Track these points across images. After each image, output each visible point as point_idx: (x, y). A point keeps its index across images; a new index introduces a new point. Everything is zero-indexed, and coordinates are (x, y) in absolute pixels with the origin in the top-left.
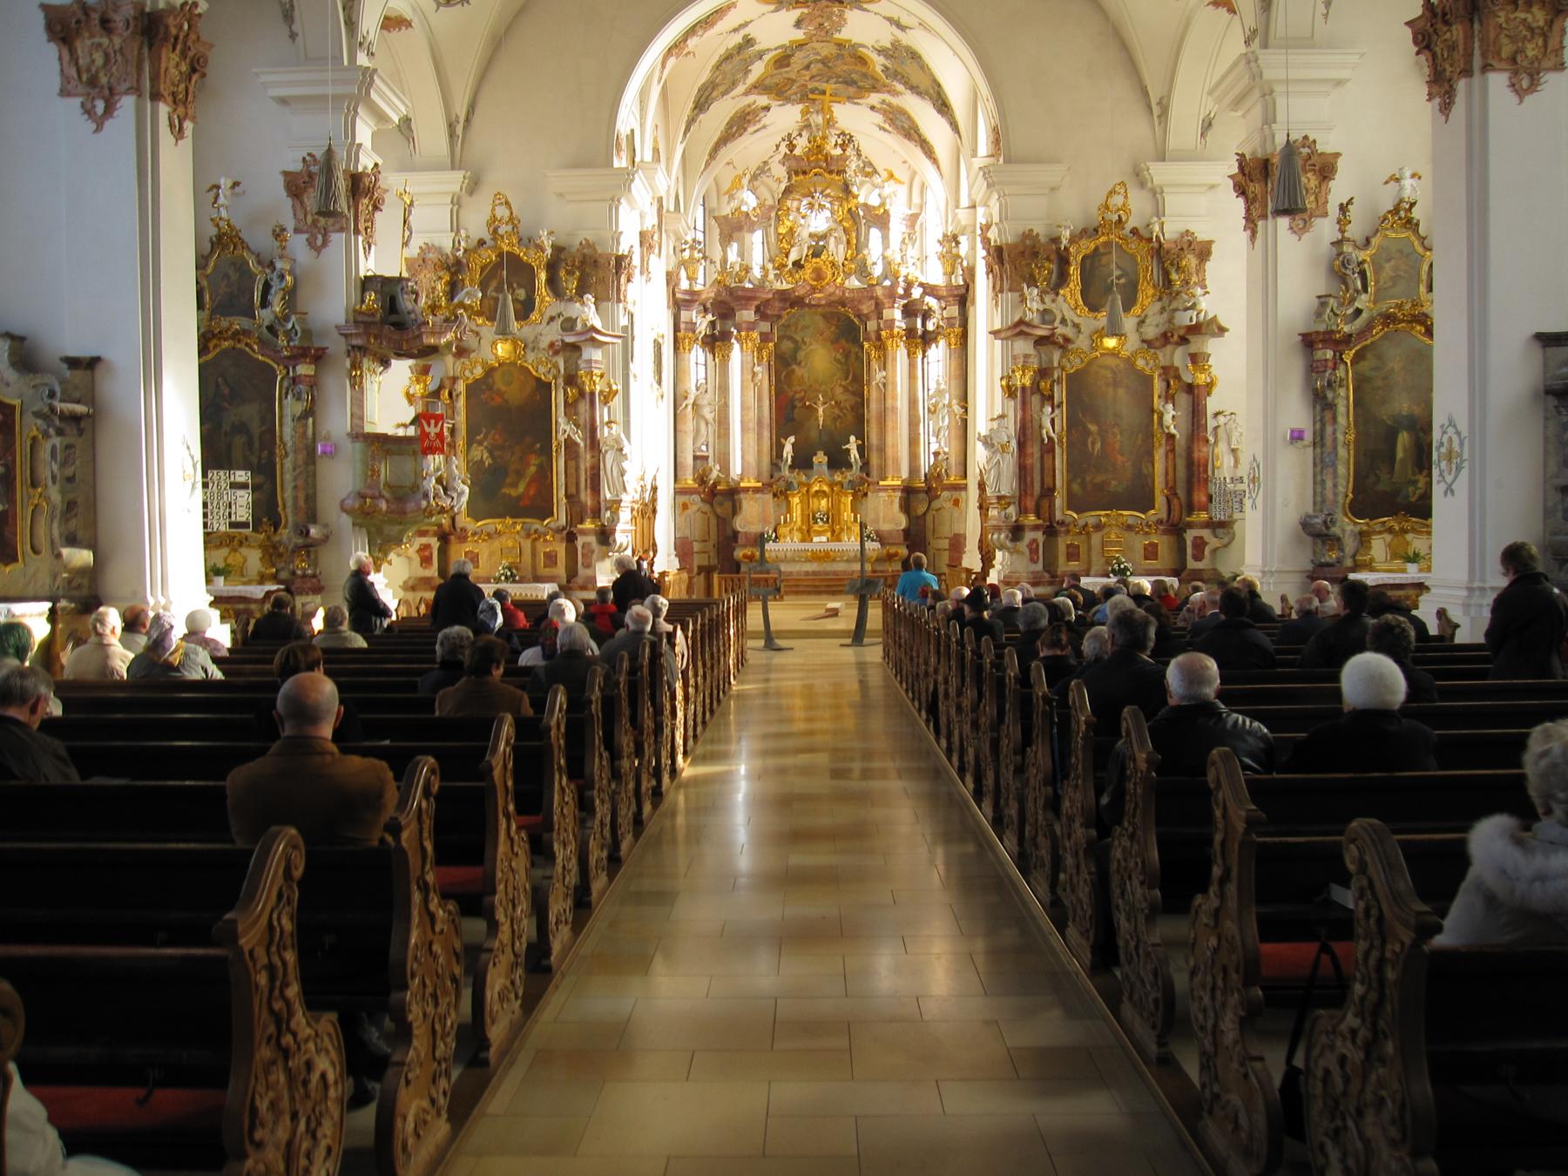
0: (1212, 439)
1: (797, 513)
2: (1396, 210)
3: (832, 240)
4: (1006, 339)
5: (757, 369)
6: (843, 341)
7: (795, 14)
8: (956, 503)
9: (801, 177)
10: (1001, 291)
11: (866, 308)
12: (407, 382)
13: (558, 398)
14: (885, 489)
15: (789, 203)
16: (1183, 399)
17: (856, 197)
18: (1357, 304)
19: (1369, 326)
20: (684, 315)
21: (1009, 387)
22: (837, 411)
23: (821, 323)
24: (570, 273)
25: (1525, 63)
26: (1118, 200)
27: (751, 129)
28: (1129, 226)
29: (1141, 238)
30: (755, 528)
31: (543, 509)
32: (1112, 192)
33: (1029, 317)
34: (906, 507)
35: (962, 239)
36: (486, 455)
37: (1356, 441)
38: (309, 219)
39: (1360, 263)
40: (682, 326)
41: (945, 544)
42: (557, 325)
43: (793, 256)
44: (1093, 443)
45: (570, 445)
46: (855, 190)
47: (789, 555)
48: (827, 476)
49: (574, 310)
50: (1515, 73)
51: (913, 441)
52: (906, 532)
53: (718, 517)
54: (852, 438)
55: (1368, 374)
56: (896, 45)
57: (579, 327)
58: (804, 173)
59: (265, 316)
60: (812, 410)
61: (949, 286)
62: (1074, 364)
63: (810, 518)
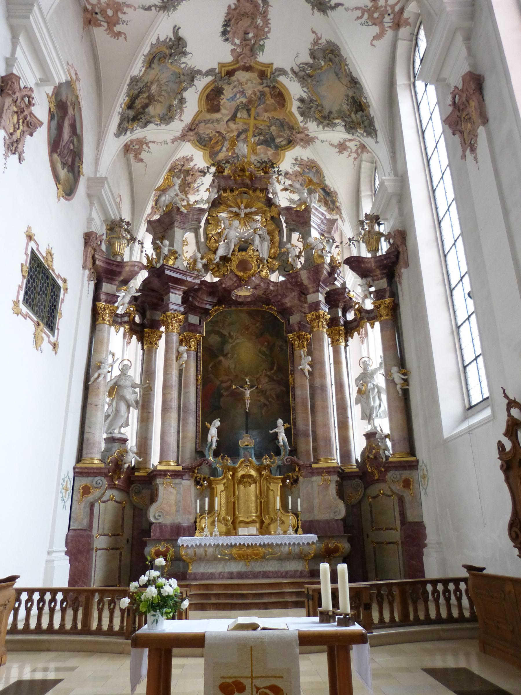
1: (220, 502)
5: (183, 348)
8: (407, 484)
14: (320, 472)
17: (276, 206)
20: (106, 287)
22: (263, 400)
23: (245, 319)
34: (341, 494)
40: (103, 297)
41: (396, 535)
43: (221, 252)
47: (210, 551)
54: (280, 422)
58: (232, 191)
60: (239, 397)
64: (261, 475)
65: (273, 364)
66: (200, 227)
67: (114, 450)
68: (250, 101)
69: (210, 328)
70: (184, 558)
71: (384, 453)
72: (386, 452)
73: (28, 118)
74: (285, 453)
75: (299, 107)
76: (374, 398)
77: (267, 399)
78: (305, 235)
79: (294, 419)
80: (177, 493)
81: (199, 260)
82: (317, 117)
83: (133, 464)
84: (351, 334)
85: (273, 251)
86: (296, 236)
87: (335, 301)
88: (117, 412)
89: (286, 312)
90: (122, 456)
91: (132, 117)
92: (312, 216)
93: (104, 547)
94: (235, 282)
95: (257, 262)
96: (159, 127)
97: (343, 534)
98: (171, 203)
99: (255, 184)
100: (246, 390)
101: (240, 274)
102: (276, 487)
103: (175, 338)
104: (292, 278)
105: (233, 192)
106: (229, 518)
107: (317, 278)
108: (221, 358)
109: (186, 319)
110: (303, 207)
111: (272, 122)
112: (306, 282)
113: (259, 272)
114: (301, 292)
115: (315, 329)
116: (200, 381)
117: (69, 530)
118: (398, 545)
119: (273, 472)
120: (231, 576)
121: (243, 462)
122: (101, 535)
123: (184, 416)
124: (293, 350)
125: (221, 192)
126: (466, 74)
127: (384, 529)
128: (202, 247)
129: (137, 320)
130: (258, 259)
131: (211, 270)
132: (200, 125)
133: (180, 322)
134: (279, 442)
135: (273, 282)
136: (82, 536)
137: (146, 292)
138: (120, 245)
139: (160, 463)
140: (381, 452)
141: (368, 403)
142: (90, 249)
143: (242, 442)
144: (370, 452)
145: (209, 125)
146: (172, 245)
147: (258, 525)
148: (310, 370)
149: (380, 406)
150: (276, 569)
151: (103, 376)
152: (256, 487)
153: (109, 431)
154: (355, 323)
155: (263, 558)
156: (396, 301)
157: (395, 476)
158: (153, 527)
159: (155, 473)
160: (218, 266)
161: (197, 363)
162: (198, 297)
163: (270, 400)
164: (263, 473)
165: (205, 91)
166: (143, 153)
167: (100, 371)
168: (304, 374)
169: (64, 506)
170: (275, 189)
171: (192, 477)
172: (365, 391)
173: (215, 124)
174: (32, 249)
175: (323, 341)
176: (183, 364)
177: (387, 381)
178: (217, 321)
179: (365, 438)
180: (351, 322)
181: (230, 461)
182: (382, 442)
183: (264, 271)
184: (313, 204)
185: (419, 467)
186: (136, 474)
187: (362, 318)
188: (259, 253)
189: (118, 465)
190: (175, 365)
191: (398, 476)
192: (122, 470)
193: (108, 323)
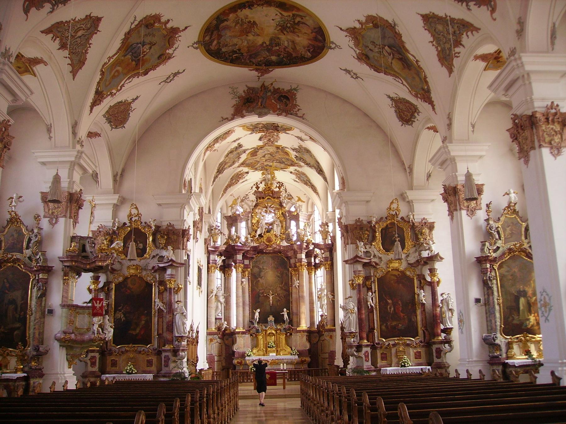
0: (441, 305)
2: (509, 207)
3: (275, 225)
4: (351, 264)
5: (243, 280)
7: (260, 135)
8: (331, 337)
9: (262, 200)
10: (348, 244)
11: (290, 254)
12: (89, 284)
13: (155, 291)
14: (300, 331)
15: (257, 211)
16: (428, 289)
17: (285, 208)
18: (497, 245)
19: (504, 254)
21: (353, 284)
22: (278, 298)
23: (271, 261)
24: (162, 237)
25: (555, 144)
26: (394, 206)
27: (241, 181)
28: (400, 216)
29: (405, 221)
30: (241, 350)
31: (147, 340)
32: (392, 203)
33: (360, 254)
34: (309, 339)
35: (330, 225)
36: (122, 316)
37: (503, 302)
38: (50, 212)
39: (497, 228)
40: (211, 262)
41: (327, 355)
42: (156, 259)
43: (259, 232)
44: (390, 308)
45: (160, 310)
46: (284, 205)
49: (164, 253)
50: (552, 148)
51: (312, 311)
53: (226, 345)
54: (285, 310)
55: (507, 274)
56: (300, 147)
57: (165, 261)
58: (263, 198)
59: (28, 252)
61: (325, 244)
62: (379, 274)
63: (267, 346)
89: (289, 258)
102: (283, 337)
108: (259, 279)
110: (296, 213)
128: (250, 229)
190: (241, 287)
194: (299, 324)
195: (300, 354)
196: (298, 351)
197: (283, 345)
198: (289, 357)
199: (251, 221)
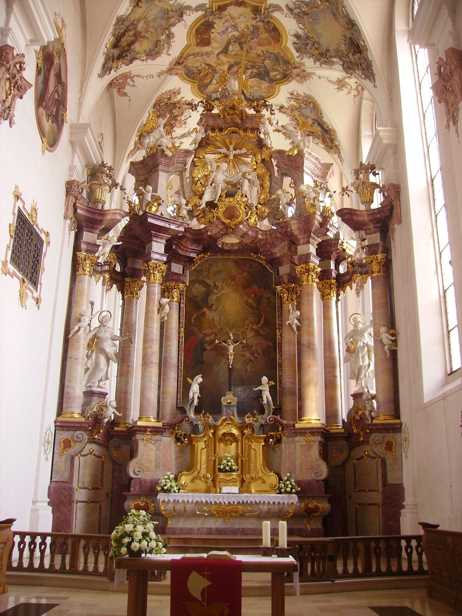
5: (165, 300)
6: (255, 287)
8: (389, 446)
14: (303, 432)
17: (268, 148)
20: (87, 236)
22: (248, 355)
34: (325, 455)
40: (83, 246)
41: (377, 497)
43: (207, 197)
47: (189, 507)
48: (237, 419)
51: (330, 385)
52: (326, 481)
53: (114, 462)
54: (265, 379)
58: (221, 130)
63: (217, 469)
64: (243, 434)
65: (260, 317)
66: (186, 169)
67: (93, 404)
68: (243, 35)
69: (194, 277)
70: (163, 513)
71: (370, 414)
72: (372, 413)
73: (19, 81)
74: (269, 411)
75: (294, 43)
76: (363, 357)
77: (252, 354)
78: (298, 181)
79: (280, 376)
80: (157, 450)
81: (184, 206)
82: (314, 53)
83: (112, 418)
84: (342, 287)
85: (263, 197)
86: (287, 181)
87: (327, 253)
88: (97, 365)
89: (275, 262)
90: (102, 410)
91: (117, 56)
92: (305, 161)
93: (84, 500)
94: (222, 230)
95: (245, 208)
96: (145, 63)
97: (324, 495)
98: (155, 145)
99: (246, 123)
100: (229, 345)
101: (227, 221)
103: (157, 289)
104: (282, 227)
105: (222, 131)
106: (209, 476)
107: (307, 229)
108: (205, 310)
109: (169, 269)
110: (296, 152)
111: (266, 55)
112: (296, 232)
113: (247, 219)
114: (291, 241)
115: (305, 283)
116: (182, 334)
117: (51, 482)
118: (379, 506)
119: (255, 430)
120: (210, 531)
121: (224, 420)
122: (81, 488)
123: (164, 370)
124: (281, 303)
125: (210, 132)
126: (448, 50)
127: (367, 490)
129: (118, 268)
130: (246, 205)
131: (196, 216)
132: (188, 58)
133: (163, 272)
134: (263, 400)
135: (262, 230)
136: (64, 488)
137: (128, 240)
138: (102, 192)
139: (140, 418)
140: (367, 413)
141: (357, 362)
142: (71, 197)
143: (224, 399)
144: (357, 413)
145: (198, 58)
146: (155, 190)
147: (238, 483)
148: (299, 324)
149: (369, 365)
150: (255, 527)
151: (83, 329)
152: (237, 446)
153: (88, 385)
154: (348, 277)
155: (242, 515)
156: (389, 258)
157: (378, 438)
158: (132, 482)
159: (135, 428)
160: (204, 212)
161: (179, 314)
162: (181, 245)
163: (255, 355)
164: (245, 431)
165: (194, 26)
166: (127, 87)
167: (80, 324)
168: (292, 329)
169: (47, 459)
170: (267, 129)
171: (172, 434)
172: (354, 350)
173: (205, 57)
174: (19, 208)
175: (312, 296)
176: (164, 317)
177: (375, 341)
178: (201, 270)
179: (352, 398)
180: (344, 275)
181: (211, 419)
182: (368, 403)
183: (253, 219)
184: (306, 149)
185: (402, 430)
186: (116, 429)
187: (354, 272)
188: (248, 199)
189: (97, 419)
191: (381, 438)
192: (101, 425)
193: (88, 274)
194: (300, 413)
195: (304, 491)
196: (298, 483)
197: (258, 467)
198: (274, 497)
199: (191, 172)
